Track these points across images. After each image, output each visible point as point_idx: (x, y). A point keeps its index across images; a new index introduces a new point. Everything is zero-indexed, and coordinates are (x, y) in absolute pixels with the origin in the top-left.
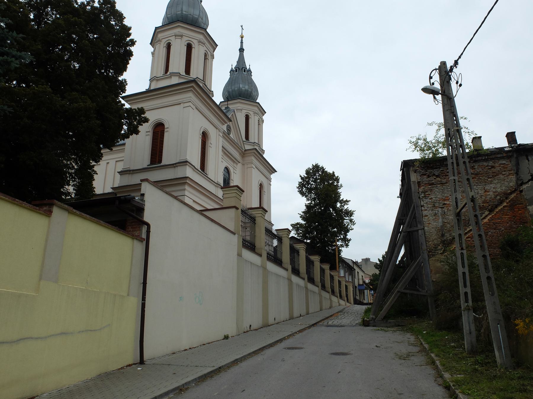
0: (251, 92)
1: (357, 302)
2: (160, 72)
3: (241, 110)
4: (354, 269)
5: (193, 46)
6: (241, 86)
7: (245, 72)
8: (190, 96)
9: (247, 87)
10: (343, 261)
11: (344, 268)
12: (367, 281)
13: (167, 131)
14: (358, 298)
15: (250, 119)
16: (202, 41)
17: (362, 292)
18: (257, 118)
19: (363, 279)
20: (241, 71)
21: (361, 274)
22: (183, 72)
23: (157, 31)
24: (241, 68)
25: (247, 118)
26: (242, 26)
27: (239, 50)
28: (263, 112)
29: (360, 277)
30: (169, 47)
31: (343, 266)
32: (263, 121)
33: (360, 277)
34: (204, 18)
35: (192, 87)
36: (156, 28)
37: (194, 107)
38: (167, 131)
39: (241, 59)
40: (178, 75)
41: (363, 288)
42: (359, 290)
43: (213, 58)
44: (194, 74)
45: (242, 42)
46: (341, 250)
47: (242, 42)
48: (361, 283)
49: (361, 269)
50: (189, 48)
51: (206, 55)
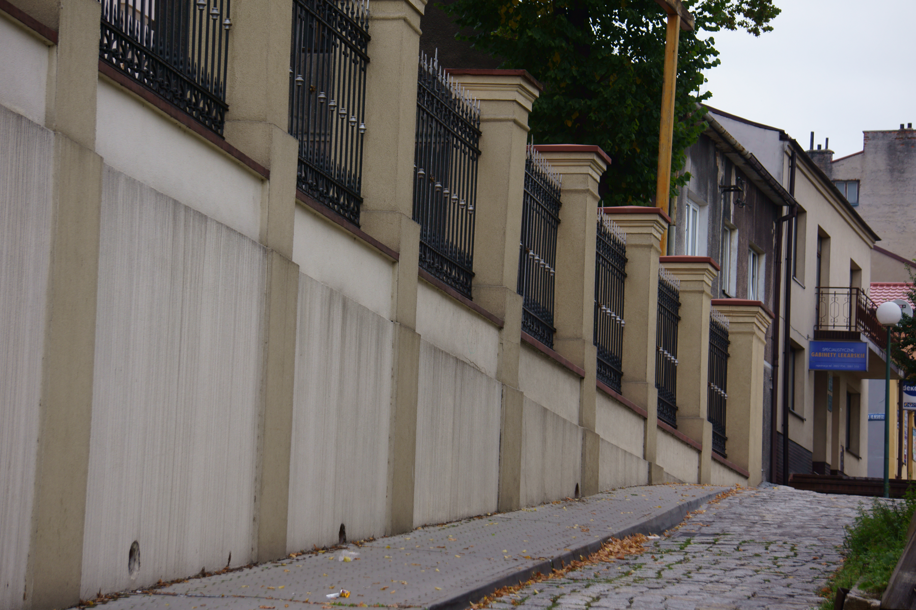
1: (790, 466)
4: (798, 212)
10: (710, 138)
11: (714, 194)
12: (891, 309)
14: (802, 434)
17: (837, 392)
19: (855, 291)
21: (846, 247)
29: (839, 276)
31: (706, 176)
33: (839, 276)
41: (844, 358)
42: (820, 377)
46: (706, 49)
48: (839, 316)
49: (849, 210)
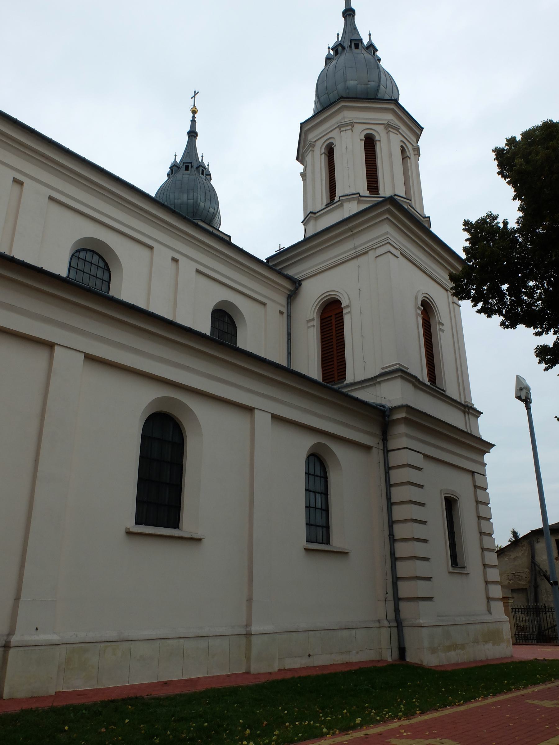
2: (321, 199)
5: (377, 138)
18: (396, 140)
22: (364, 190)
30: (330, 152)
40: (358, 197)
43: (419, 155)
44: (385, 191)
51: (403, 150)
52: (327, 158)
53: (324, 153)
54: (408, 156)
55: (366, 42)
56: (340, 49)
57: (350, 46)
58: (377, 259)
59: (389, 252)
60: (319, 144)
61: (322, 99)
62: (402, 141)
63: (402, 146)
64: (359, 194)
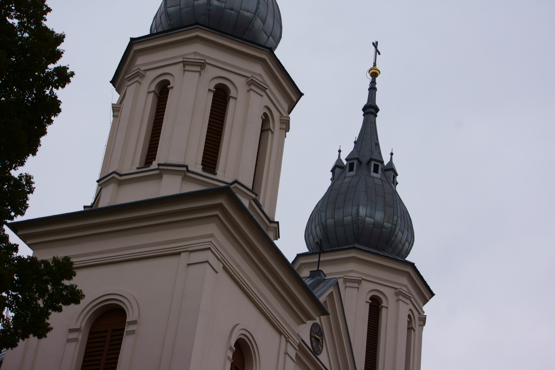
0: (392, 231)
2: (131, 162)
3: (359, 282)
6: (362, 211)
7: (376, 171)
8: (211, 232)
9: (379, 216)
13: (133, 332)
15: (384, 311)
16: (258, 79)
20: (365, 171)
23: (136, 48)
24: (365, 160)
25: (375, 306)
26: (375, 45)
27: (364, 109)
28: (426, 293)
30: (163, 92)
32: (423, 320)
34: (270, 21)
35: (219, 206)
36: (133, 41)
37: (219, 266)
38: (133, 332)
39: (368, 136)
44: (225, 172)
45: (373, 89)
47: (373, 89)
50: (221, 97)
51: (266, 120)
52: (156, 99)
53: (154, 91)
54: (270, 129)
55: (386, 161)
56: (356, 162)
57: (369, 163)
58: (190, 267)
59: (207, 262)
60: (151, 75)
61: (170, 10)
62: (411, 310)
63: (409, 316)
64: (187, 167)
